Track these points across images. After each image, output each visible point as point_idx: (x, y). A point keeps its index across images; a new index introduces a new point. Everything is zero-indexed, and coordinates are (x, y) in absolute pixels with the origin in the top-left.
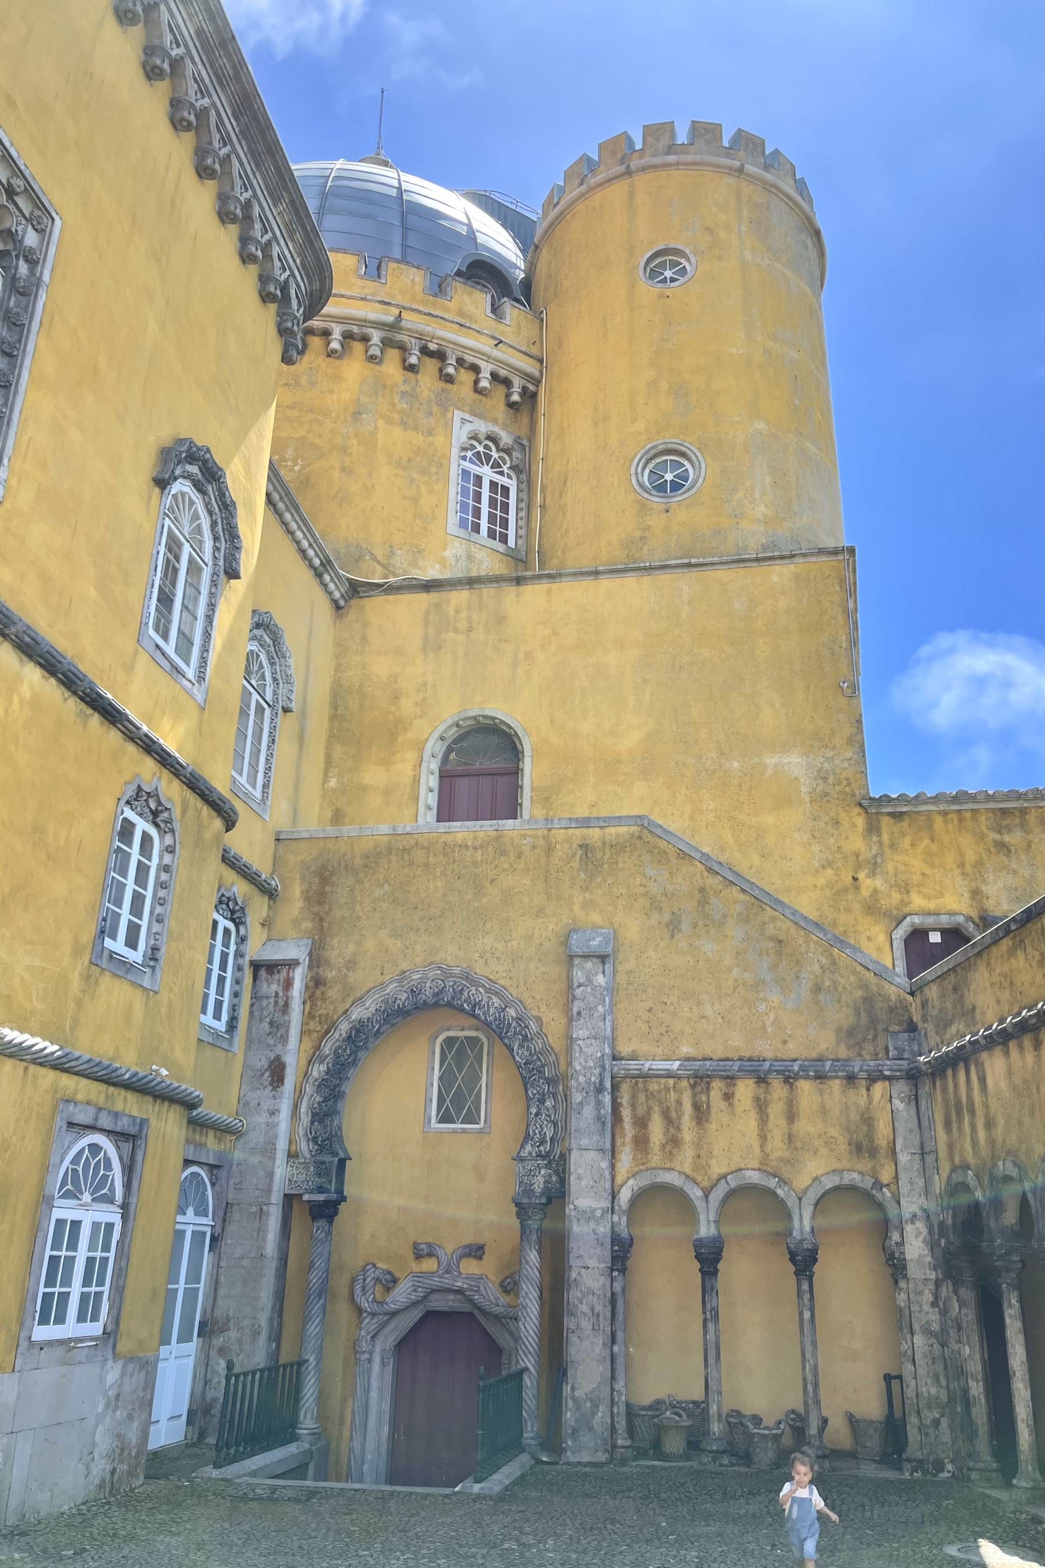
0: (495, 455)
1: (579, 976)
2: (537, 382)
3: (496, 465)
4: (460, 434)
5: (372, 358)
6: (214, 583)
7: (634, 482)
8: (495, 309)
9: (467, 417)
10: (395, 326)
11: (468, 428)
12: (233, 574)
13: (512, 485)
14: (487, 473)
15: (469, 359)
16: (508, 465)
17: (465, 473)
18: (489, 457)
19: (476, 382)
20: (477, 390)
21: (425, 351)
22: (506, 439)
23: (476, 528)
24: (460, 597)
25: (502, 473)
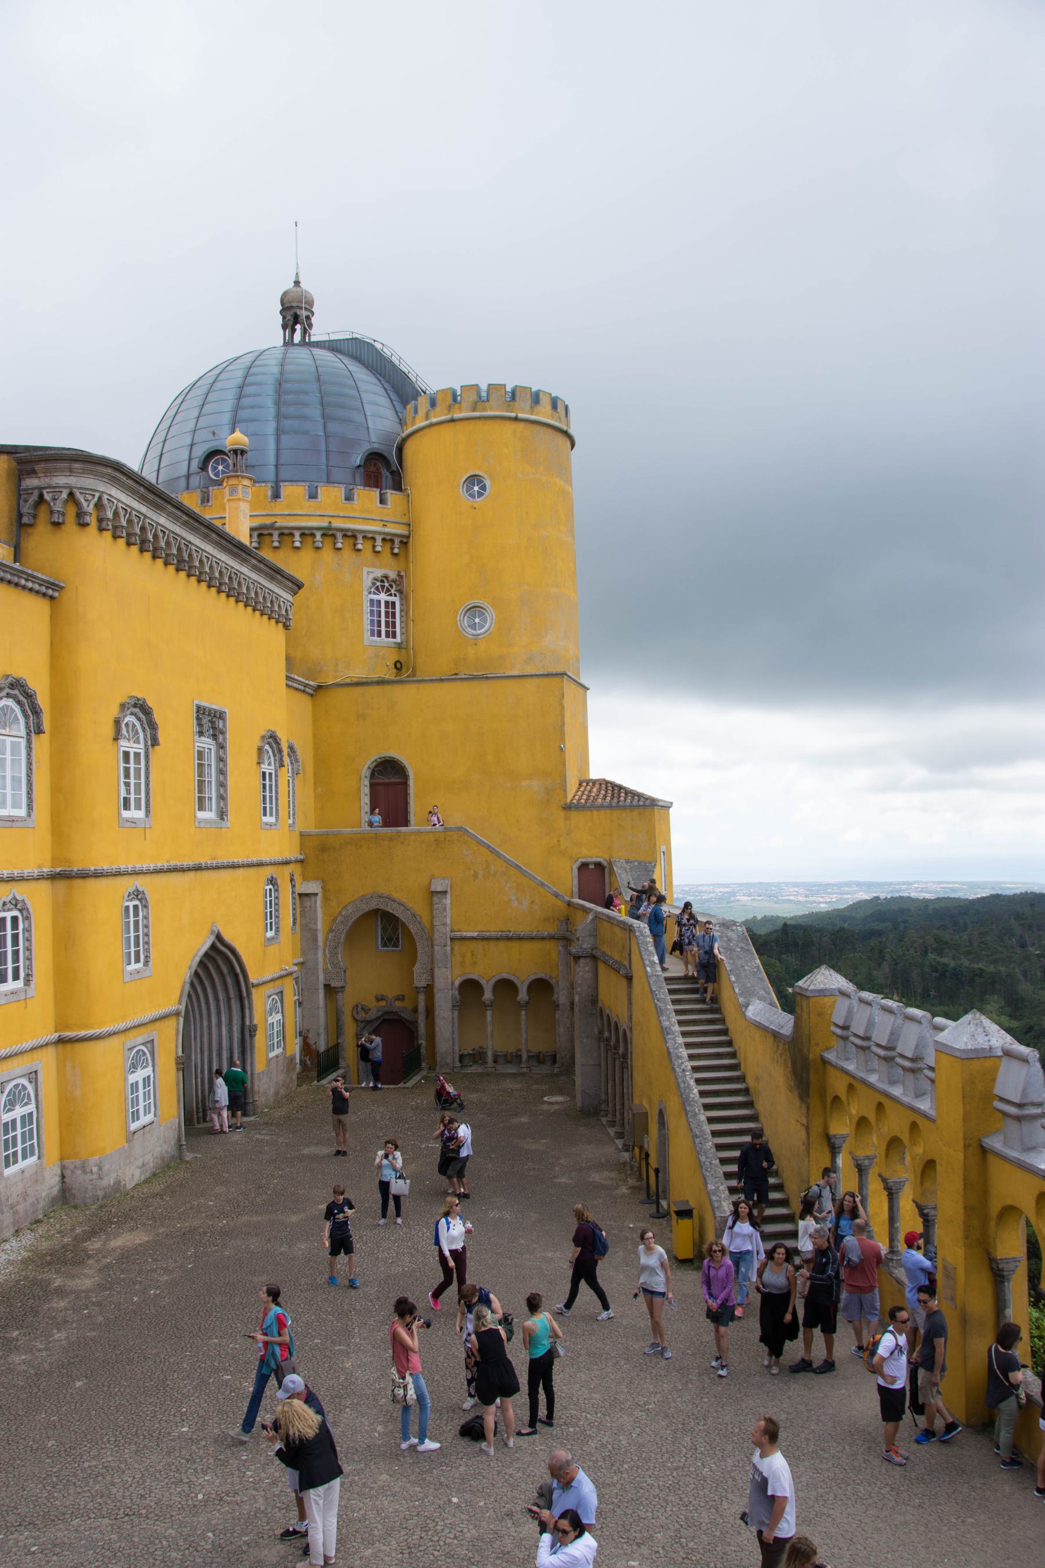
0: (386, 584)
1: (435, 899)
2: (408, 537)
3: (388, 590)
4: (367, 581)
5: (318, 548)
6: (276, 776)
8: (382, 501)
9: (371, 570)
10: (329, 528)
11: (372, 576)
12: (282, 766)
13: (397, 600)
14: (383, 597)
17: (372, 601)
18: (383, 587)
19: (374, 547)
21: (345, 536)
22: (393, 575)
23: (379, 632)
25: (391, 595)
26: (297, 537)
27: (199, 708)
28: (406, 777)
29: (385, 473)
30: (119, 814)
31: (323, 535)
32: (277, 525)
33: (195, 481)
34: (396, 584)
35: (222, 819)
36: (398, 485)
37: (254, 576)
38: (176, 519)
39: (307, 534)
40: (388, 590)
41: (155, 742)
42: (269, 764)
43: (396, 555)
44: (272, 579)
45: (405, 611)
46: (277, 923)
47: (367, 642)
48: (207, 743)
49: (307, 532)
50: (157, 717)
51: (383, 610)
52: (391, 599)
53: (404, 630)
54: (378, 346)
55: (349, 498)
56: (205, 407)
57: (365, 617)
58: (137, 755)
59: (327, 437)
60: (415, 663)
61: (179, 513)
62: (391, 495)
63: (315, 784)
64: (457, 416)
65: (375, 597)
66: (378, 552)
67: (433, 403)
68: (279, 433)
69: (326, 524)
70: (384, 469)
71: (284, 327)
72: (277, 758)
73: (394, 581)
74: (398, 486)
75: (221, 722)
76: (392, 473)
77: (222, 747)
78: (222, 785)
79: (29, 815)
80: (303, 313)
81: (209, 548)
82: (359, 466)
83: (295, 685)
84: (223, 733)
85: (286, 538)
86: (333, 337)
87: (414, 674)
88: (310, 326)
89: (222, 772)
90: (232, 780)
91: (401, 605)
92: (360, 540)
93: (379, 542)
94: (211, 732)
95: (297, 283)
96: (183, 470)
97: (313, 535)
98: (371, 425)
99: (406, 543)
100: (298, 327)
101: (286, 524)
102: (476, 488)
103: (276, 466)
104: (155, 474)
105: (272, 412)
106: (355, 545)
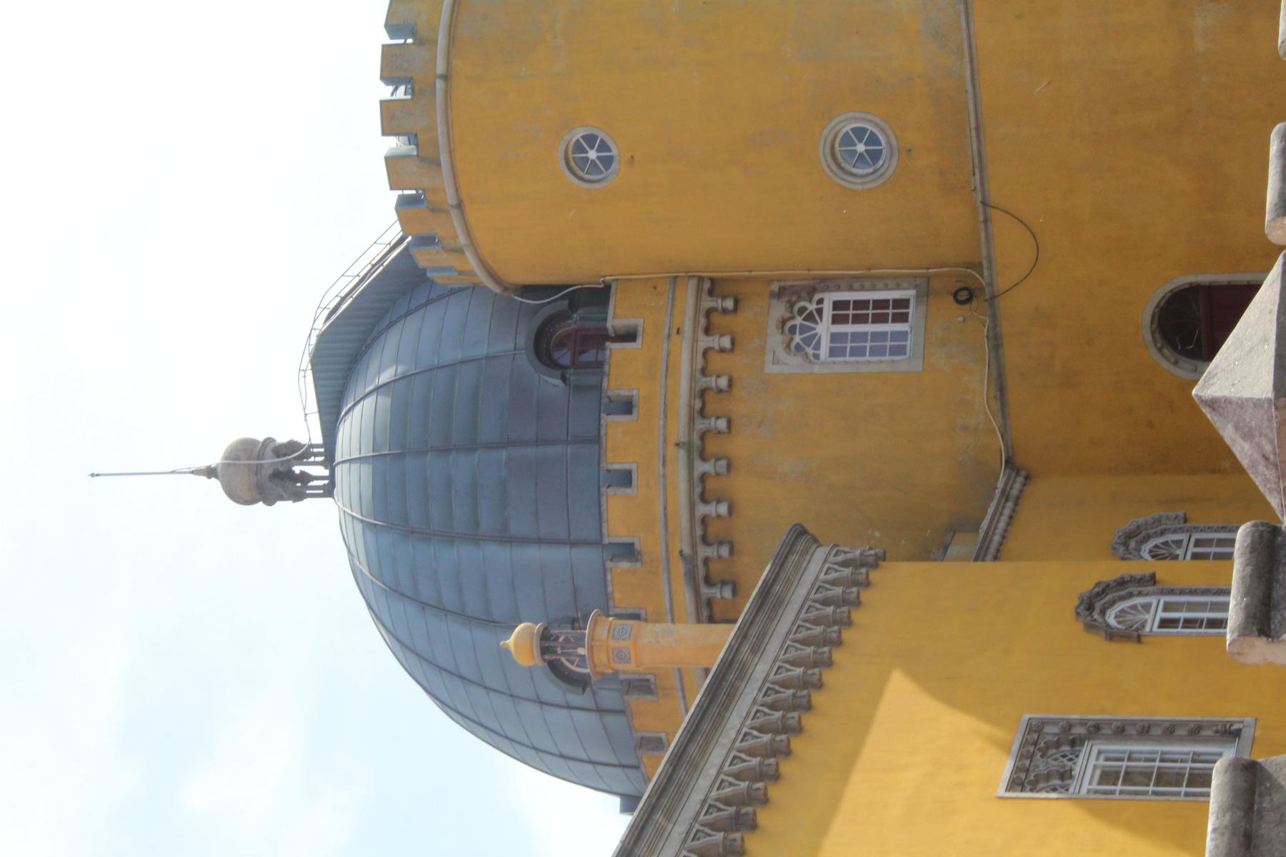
2: (701, 279)
4: (793, 364)
5: (729, 467)
6: (1171, 592)
7: (872, 185)
8: (629, 336)
10: (688, 446)
11: (782, 355)
12: (1152, 579)
13: (830, 298)
14: (824, 328)
15: (700, 362)
16: (807, 304)
17: (833, 352)
19: (722, 350)
24: (1013, 354)
25: (820, 311)
26: (710, 509)
28: (1194, 289)
29: (574, 322)
31: (704, 458)
32: (687, 551)
33: (609, 698)
34: (797, 293)
35: (1237, 734)
36: (599, 296)
37: (772, 648)
38: (660, 832)
39: (703, 491)
40: (810, 317)
42: (1147, 607)
43: (736, 302)
44: (780, 603)
45: (852, 283)
47: (917, 366)
48: (1089, 762)
49: (698, 490)
51: (849, 328)
53: (891, 284)
54: (321, 326)
55: (627, 407)
56: (464, 672)
57: (863, 369)
59: (509, 443)
60: (957, 265)
61: (650, 829)
62: (616, 319)
63: (1213, 471)
64: (451, 199)
65: (824, 351)
66: (733, 342)
67: (426, 241)
68: (506, 539)
69: (682, 453)
70: (567, 326)
71: (298, 496)
72: (1135, 589)
73: (792, 305)
74: (599, 296)
75: (1048, 729)
76: (573, 307)
77: (1095, 730)
78: (1170, 731)
80: (270, 460)
81: (716, 757)
82: (564, 379)
83: (1002, 525)
84: (1070, 725)
85: (711, 530)
86: (313, 406)
87: (977, 266)
88: (292, 446)
89: (1145, 730)
90: (1166, 712)
91: (838, 289)
92: (711, 381)
94: (1066, 748)
95: (210, 472)
96: (592, 718)
97: (703, 477)
98: (482, 351)
99: (712, 280)
100: (297, 469)
101: (685, 533)
102: (592, 154)
103: (573, 544)
104: (599, 768)
105: (465, 551)
106: (720, 391)
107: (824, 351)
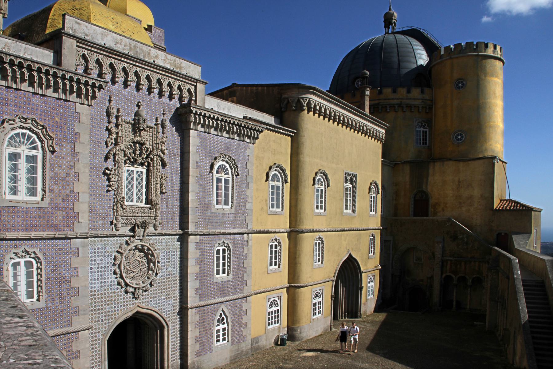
13: (427, 130)
14: (422, 129)
17: (417, 131)
20: (419, 112)
27: (346, 173)
30: (314, 211)
39: (392, 107)
41: (328, 186)
45: (430, 134)
46: (374, 251)
50: (329, 177)
52: (425, 130)
58: (322, 190)
65: (418, 129)
79: (282, 211)
84: (355, 182)
93: (420, 109)
97: (395, 107)
107: (418, 129)
